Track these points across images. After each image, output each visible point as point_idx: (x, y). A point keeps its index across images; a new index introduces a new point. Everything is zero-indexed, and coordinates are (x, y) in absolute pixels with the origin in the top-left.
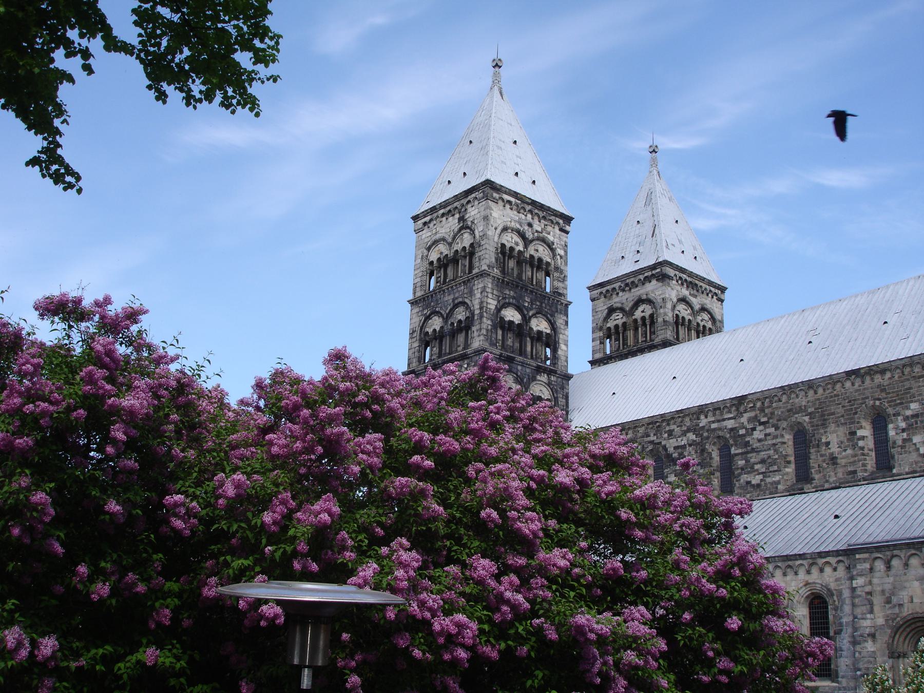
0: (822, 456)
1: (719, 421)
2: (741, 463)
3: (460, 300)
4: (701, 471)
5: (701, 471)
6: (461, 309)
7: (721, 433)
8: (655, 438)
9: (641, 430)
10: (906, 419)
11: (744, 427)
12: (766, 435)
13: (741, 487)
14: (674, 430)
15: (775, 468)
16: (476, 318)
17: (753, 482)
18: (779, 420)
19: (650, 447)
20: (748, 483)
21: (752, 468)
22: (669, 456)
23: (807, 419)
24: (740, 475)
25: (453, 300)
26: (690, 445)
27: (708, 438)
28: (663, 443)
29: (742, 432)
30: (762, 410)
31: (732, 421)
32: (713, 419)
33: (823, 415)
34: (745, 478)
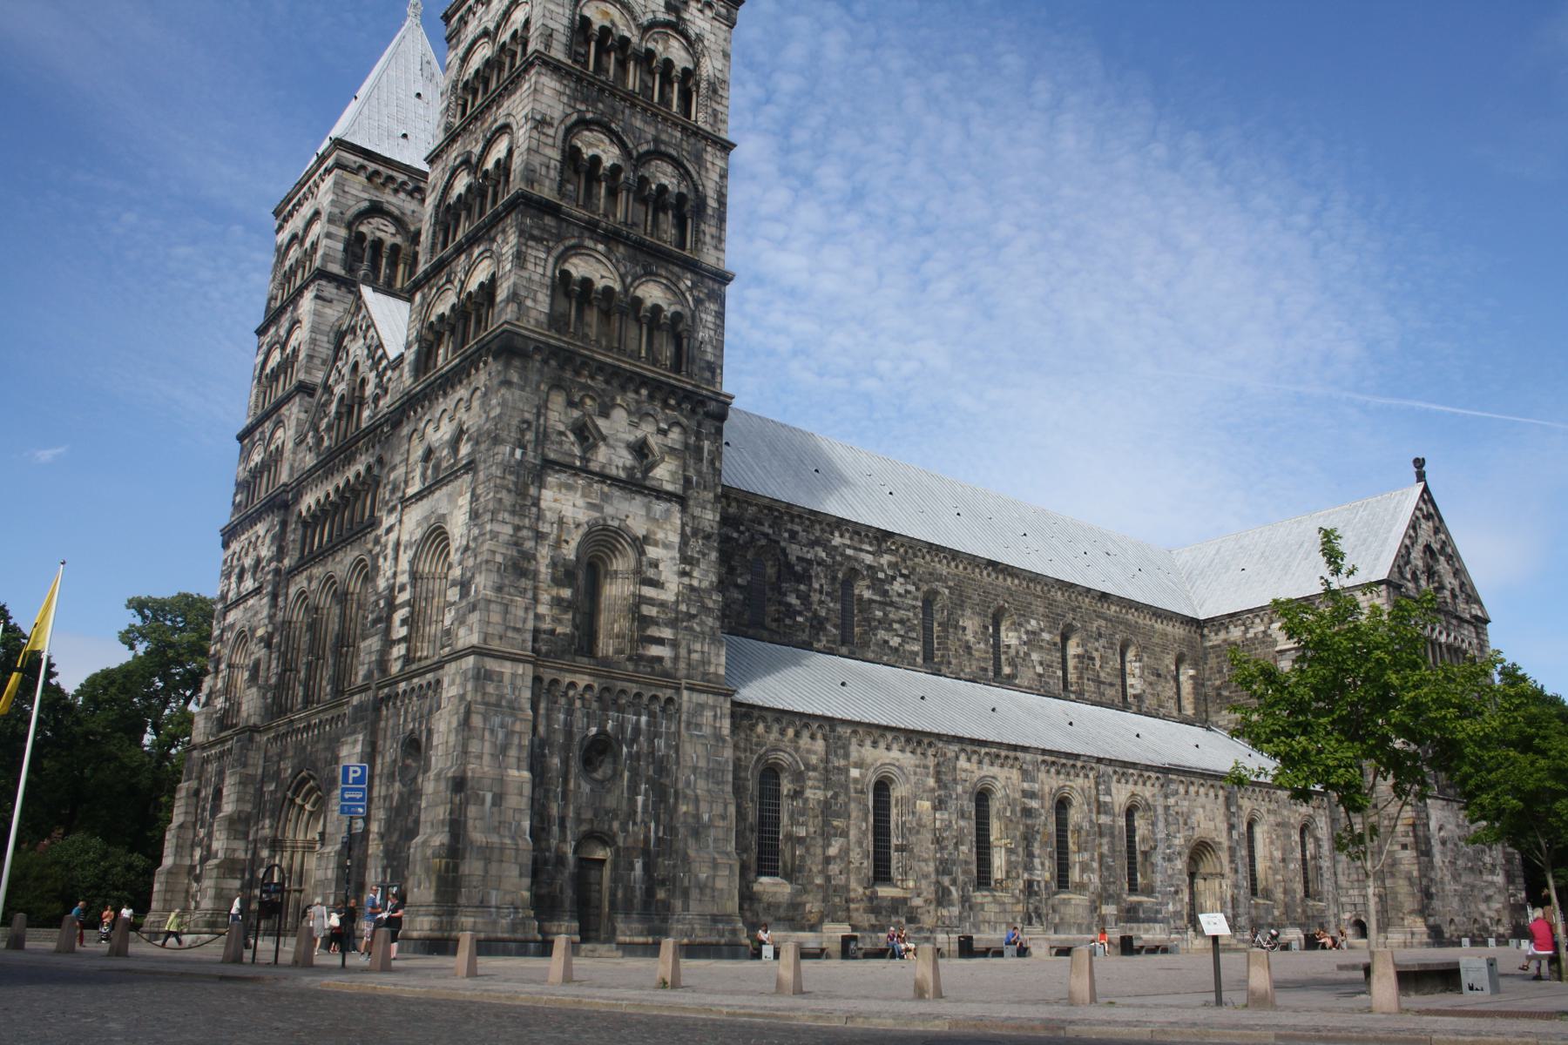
0: (959, 640)
1: (855, 549)
2: (879, 614)
3: (674, 153)
4: (831, 605)
5: (831, 605)
6: (669, 169)
7: (857, 567)
8: (771, 531)
9: (752, 510)
10: (1027, 632)
11: (883, 571)
12: (907, 592)
13: (877, 644)
14: (797, 533)
15: (914, 635)
16: (710, 211)
17: (891, 643)
18: (920, 580)
19: (763, 542)
20: (886, 642)
21: (890, 625)
22: (790, 566)
23: (947, 591)
24: (876, 628)
25: (656, 140)
26: (819, 564)
27: (841, 564)
28: (783, 544)
29: (881, 575)
30: (904, 560)
31: (871, 557)
32: (848, 542)
33: (961, 595)
34: (882, 634)
